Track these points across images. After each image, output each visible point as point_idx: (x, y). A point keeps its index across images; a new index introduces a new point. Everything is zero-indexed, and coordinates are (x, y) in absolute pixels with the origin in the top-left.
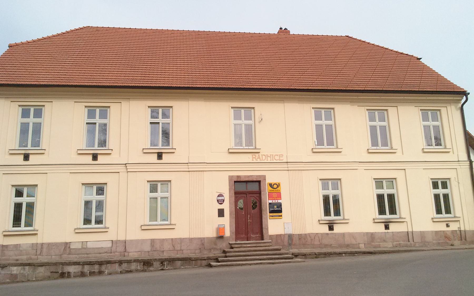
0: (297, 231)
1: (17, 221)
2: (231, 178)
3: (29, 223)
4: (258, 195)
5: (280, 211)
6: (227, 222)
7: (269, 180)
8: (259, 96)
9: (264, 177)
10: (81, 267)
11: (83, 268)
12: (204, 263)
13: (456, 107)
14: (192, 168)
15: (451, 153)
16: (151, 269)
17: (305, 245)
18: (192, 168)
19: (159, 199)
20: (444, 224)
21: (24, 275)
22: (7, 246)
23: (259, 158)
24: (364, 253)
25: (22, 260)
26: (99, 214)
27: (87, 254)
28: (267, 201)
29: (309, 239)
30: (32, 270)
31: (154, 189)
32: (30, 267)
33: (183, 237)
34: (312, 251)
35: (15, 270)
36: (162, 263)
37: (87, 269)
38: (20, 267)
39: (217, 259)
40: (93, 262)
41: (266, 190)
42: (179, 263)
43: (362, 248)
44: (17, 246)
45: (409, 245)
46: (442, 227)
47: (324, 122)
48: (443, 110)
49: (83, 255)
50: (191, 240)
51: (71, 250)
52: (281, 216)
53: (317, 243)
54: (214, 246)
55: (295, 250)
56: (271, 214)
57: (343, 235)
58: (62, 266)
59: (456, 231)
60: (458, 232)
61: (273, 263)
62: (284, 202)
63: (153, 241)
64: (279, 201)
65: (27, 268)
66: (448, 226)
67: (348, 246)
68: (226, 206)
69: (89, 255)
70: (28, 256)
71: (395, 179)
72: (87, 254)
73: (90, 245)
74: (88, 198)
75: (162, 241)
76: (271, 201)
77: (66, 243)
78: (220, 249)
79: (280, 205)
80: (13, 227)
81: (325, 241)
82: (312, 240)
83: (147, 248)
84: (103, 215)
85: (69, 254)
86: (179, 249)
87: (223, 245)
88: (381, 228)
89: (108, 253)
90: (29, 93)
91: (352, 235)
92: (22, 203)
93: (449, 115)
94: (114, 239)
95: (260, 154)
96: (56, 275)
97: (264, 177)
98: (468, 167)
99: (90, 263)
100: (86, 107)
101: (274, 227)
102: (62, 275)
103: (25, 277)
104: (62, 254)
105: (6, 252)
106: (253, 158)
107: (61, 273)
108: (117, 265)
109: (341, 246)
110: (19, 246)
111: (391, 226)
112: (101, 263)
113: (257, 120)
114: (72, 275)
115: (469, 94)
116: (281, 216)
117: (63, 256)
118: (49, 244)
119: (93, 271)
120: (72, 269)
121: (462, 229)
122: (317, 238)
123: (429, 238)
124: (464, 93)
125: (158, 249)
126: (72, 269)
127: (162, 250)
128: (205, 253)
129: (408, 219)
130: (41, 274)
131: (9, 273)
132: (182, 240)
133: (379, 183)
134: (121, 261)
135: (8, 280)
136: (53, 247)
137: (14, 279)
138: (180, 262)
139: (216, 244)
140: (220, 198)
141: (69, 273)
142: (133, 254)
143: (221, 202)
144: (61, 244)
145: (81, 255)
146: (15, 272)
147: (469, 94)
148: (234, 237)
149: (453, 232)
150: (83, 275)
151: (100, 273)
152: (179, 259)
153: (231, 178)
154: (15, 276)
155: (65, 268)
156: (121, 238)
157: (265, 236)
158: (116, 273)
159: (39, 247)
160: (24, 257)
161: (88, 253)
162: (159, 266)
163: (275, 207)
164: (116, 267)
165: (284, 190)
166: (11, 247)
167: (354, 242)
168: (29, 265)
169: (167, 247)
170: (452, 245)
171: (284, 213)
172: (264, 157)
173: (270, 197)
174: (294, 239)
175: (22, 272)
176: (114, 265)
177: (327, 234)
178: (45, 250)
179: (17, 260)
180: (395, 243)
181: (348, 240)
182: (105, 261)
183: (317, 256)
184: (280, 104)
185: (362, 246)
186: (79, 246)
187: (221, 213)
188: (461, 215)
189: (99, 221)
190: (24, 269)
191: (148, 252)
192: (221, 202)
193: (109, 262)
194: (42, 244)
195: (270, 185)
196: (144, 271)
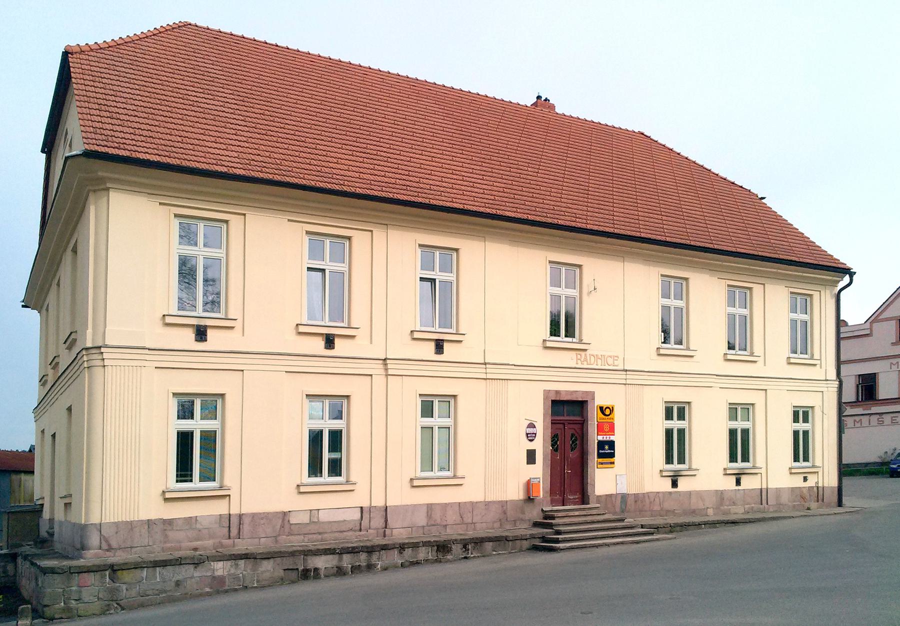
0: (633, 491)
1: (184, 471)
2: (547, 393)
3: (208, 475)
4: (579, 426)
5: (612, 455)
6: (538, 471)
7: (601, 400)
8: (594, 244)
9: (592, 394)
10: (337, 557)
11: (340, 560)
12: (526, 544)
13: (831, 292)
14: (492, 372)
15: (818, 366)
16: (449, 557)
17: (641, 512)
18: (489, 371)
19: (436, 430)
20: (801, 477)
21: (236, 578)
22: (169, 523)
23: (586, 360)
24: (713, 524)
25: (205, 549)
26: (335, 455)
27: (320, 533)
28: (594, 437)
29: (647, 501)
30: (250, 566)
31: (427, 410)
32: (248, 561)
33: (475, 500)
34: (666, 522)
35: (220, 568)
36: (465, 546)
37: (347, 561)
38: (229, 563)
39: (543, 537)
40: (357, 548)
41: (594, 418)
42: (489, 546)
43: (711, 515)
44: (190, 521)
45: (763, 511)
46: (798, 482)
47: (673, 303)
48: (757, 289)
49: (315, 536)
50: (487, 504)
51: (292, 527)
52: (613, 463)
53: (657, 508)
54: (521, 516)
55: (635, 522)
56: (600, 460)
57: (689, 494)
58: (299, 560)
59: (812, 487)
60: (815, 489)
61: (637, 542)
62: (618, 438)
63: (430, 507)
64: (612, 438)
65: (242, 563)
66: (805, 479)
67: (693, 512)
68: (540, 445)
69: (326, 535)
70: (217, 541)
71: (753, 404)
72: (320, 533)
73: (324, 517)
74: (317, 425)
75: (445, 506)
76: (600, 438)
77: (285, 514)
78: (529, 520)
79: (612, 444)
80: (177, 481)
81: (667, 505)
82: (651, 503)
83: (421, 520)
84: (341, 459)
85: (290, 534)
86: (470, 521)
87: (534, 514)
88: (729, 484)
89: (355, 531)
90: (116, 176)
91: (700, 494)
92: (192, 433)
93: (823, 302)
94: (366, 504)
95: (588, 353)
96: (294, 575)
97: (592, 394)
98: (836, 390)
99: (353, 551)
100: (176, 216)
101: (604, 481)
102: (306, 575)
103: (239, 578)
104: (279, 535)
105: (171, 534)
106: (577, 359)
107: (303, 570)
108: (396, 552)
109: (685, 513)
110: (194, 520)
111: (744, 480)
112: (370, 550)
113: (585, 291)
114: (322, 573)
115: (855, 273)
116: (613, 463)
117: (279, 538)
118: (254, 516)
119: (357, 564)
120: (321, 563)
121: (820, 485)
122: (657, 500)
123: (785, 499)
124: (847, 271)
125: (439, 521)
126: (321, 563)
127: (445, 523)
128: (508, 527)
129: (763, 471)
130: (268, 575)
131: (209, 574)
132: (473, 505)
133: (733, 411)
134: (404, 544)
135: (208, 590)
136: (262, 522)
137: (219, 587)
138: (491, 543)
139: (523, 513)
140: (531, 430)
141: (316, 570)
142: (399, 533)
143: (531, 437)
144: (276, 514)
145: (311, 536)
146: (219, 573)
147: (855, 273)
148: (549, 498)
149: (811, 488)
150: (340, 572)
151: (370, 567)
152: (490, 539)
153: (547, 393)
154: (221, 580)
155: (309, 561)
156: (378, 502)
157: (591, 499)
158: (395, 567)
159: (235, 521)
160: (209, 543)
161: (321, 531)
162: (460, 551)
163: (607, 447)
164: (395, 557)
165: (618, 418)
166: (180, 522)
167: (701, 506)
168: (246, 556)
169: (452, 517)
170: (809, 509)
171: (616, 459)
172: (592, 358)
173: (600, 429)
174: (629, 502)
175: (233, 571)
176: (391, 552)
177: (670, 493)
178: (246, 528)
179: (195, 549)
180: (747, 506)
181: (696, 504)
182: (378, 546)
183: (672, 528)
184: (500, 245)
185: (710, 512)
186: (305, 519)
187: (531, 457)
188: (764, 466)
189: (335, 468)
190: (237, 565)
191: (423, 527)
192: (531, 437)
193: (385, 548)
194: (240, 516)
195: (601, 408)
196: (438, 561)
